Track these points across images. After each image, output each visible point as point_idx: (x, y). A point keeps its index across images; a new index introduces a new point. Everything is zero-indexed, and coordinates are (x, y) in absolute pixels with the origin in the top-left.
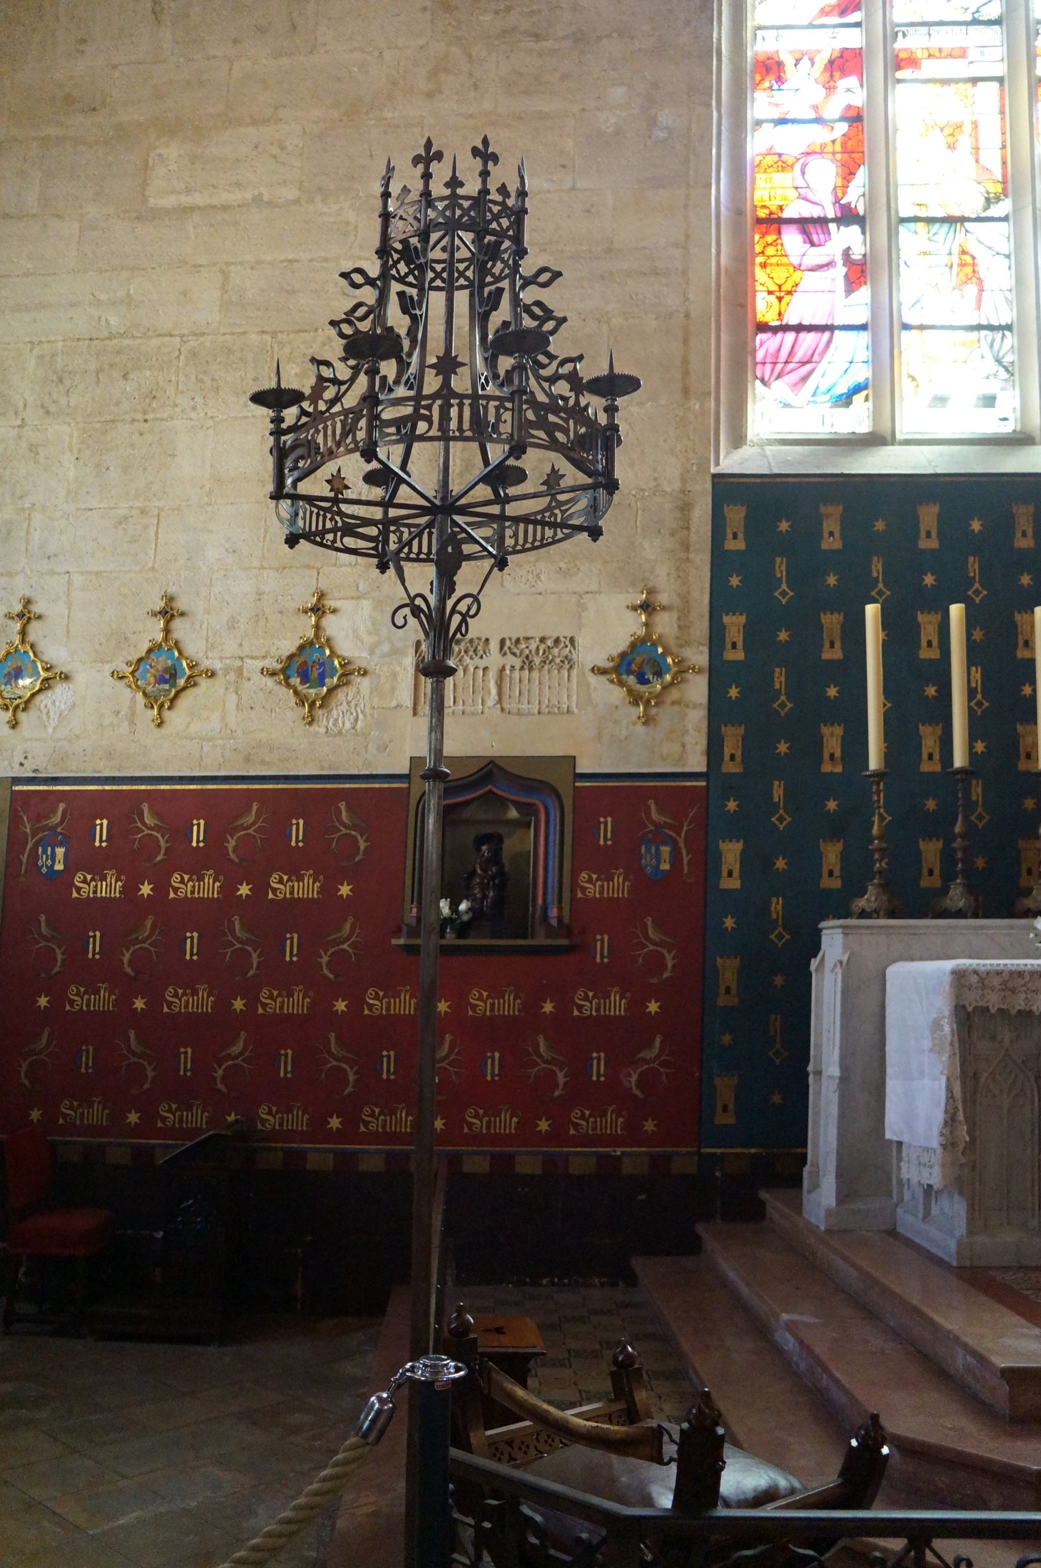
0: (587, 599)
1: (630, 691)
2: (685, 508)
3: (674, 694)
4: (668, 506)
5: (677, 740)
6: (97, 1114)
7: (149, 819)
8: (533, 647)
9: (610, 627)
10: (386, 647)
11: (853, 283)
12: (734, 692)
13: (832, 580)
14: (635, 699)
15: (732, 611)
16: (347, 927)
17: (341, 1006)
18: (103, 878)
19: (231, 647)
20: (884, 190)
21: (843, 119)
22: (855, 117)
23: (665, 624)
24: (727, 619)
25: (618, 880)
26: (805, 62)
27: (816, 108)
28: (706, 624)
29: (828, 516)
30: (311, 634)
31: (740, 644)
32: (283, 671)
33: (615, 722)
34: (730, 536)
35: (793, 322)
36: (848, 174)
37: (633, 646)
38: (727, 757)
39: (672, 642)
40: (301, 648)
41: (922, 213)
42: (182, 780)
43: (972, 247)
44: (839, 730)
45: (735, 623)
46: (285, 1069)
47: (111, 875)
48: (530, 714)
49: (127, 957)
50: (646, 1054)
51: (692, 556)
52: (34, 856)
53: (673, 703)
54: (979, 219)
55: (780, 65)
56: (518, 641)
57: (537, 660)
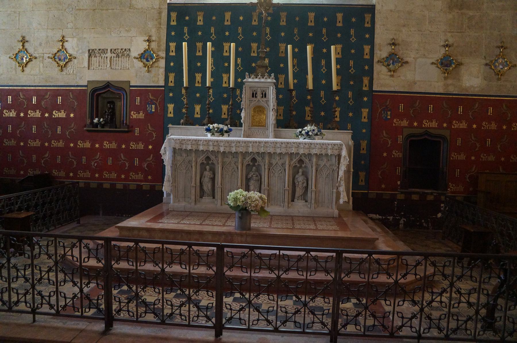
0: (133, 38)
1: (144, 64)
2: (160, 13)
3: (156, 64)
4: (156, 12)
5: (156, 77)
6: (13, 172)
7: (21, 96)
8: (119, 51)
9: (139, 46)
10: (80, 51)
12: (172, 64)
13: (200, 33)
16: (73, 125)
17: (72, 145)
18: (11, 112)
19: (40, 50)
23: (154, 45)
24: (171, 44)
25: (141, 114)
28: (165, 45)
29: (199, 15)
31: (174, 51)
33: (141, 72)
34: (172, 21)
37: (145, 51)
38: (170, 82)
39: (156, 50)
42: (30, 86)
46: (59, 161)
47: (13, 111)
48: (118, 69)
49: (18, 132)
50: (148, 159)
51: (162, 26)
53: (156, 67)
56: (115, 50)
57: (120, 55)
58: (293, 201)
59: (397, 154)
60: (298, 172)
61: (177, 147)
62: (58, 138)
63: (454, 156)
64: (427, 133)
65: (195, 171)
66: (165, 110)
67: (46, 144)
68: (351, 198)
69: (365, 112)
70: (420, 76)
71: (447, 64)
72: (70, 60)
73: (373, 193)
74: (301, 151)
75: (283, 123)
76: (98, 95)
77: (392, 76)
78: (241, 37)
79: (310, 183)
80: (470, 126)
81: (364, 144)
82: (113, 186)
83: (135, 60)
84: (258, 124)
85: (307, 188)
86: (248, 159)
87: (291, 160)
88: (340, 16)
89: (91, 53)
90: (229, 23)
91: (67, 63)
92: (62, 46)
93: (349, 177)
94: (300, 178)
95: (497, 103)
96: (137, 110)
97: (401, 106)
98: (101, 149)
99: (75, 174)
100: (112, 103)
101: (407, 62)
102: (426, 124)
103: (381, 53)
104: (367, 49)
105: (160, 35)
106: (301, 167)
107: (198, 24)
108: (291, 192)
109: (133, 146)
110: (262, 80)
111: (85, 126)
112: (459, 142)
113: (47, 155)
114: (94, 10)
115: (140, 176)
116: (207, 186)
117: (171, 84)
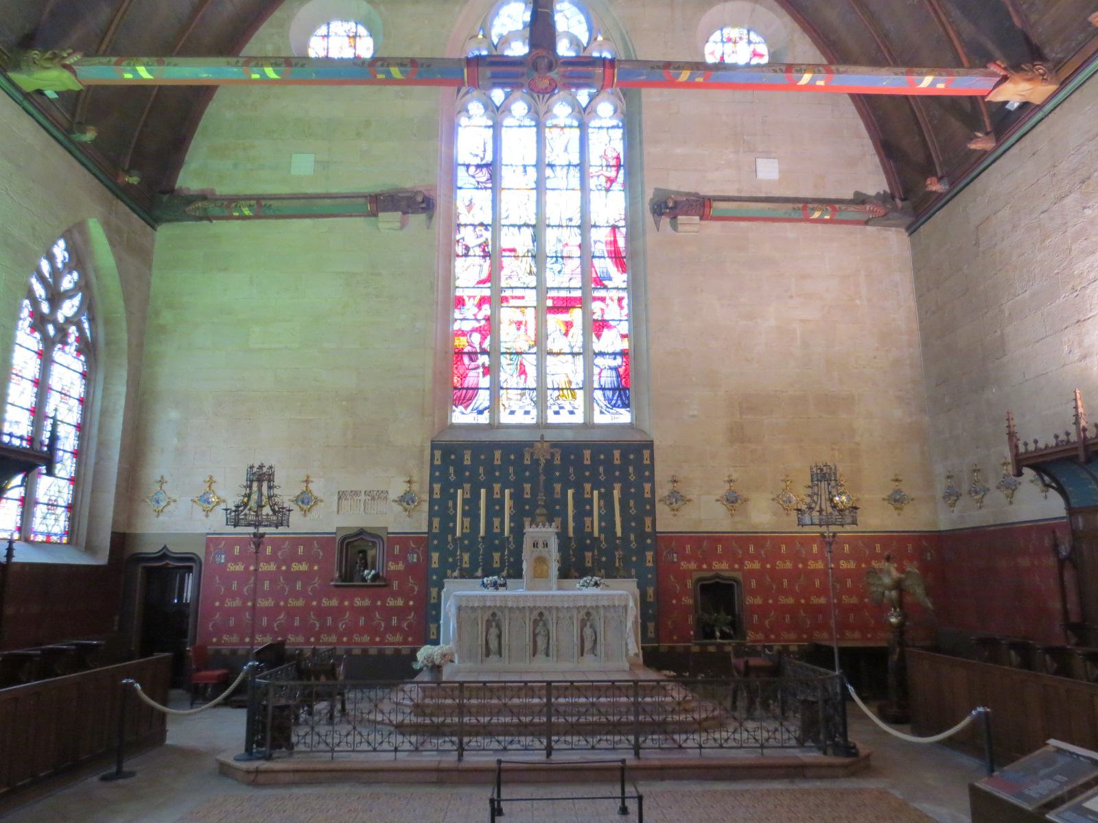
2: (422, 451)
3: (418, 508)
5: (418, 522)
6: (235, 639)
9: (398, 488)
11: (485, 374)
14: (406, 510)
20: (496, 342)
21: (484, 319)
22: (487, 319)
23: (415, 487)
26: (472, 299)
27: (475, 315)
30: (305, 489)
32: (296, 500)
35: (466, 385)
36: (484, 338)
37: (405, 494)
40: (302, 493)
41: (508, 351)
43: (525, 363)
44: (469, 519)
45: (437, 487)
50: (409, 618)
52: (214, 558)
54: (526, 353)
55: (463, 300)
58: (582, 655)
59: (688, 601)
60: (586, 625)
61: (464, 604)
62: (296, 595)
63: (750, 600)
64: (718, 576)
65: (481, 628)
66: (428, 559)
67: (282, 604)
68: (641, 651)
69: (649, 555)
70: (705, 514)
71: (733, 501)
72: (316, 503)
73: (664, 646)
74: (589, 604)
75: (564, 574)
76: (348, 544)
77: (675, 515)
78: (512, 478)
79: (598, 635)
80: (763, 566)
81: (651, 591)
82: (365, 651)
83: (393, 504)
84: (540, 575)
85: (595, 640)
86: (536, 613)
87: (579, 612)
88: (617, 453)
89: (341, 496)
90: (499, 462)
91: (311, 507)
92: (307, 487)
93: (637, 628)
94: (588, 631)
95: (789, 540)
96: (396, 559)
97: (688, 547)
98: (352, 608)
99: (318, 639)
100: (364, 552)
101: (689, 500)
102: (717, 566)
103: (662, 491)
104: (647, 487)
105: (422, 475)
106: (588, 620)
107: (465, 463)
108: (579, 646)
109: (391, 602)
110: (544, 530)
111: (332, 580)
112: (753, 583)
113: (282, 617)
114: (346, 447)
115: (399, 638)
116: (493, 645)
117: (436, 531)
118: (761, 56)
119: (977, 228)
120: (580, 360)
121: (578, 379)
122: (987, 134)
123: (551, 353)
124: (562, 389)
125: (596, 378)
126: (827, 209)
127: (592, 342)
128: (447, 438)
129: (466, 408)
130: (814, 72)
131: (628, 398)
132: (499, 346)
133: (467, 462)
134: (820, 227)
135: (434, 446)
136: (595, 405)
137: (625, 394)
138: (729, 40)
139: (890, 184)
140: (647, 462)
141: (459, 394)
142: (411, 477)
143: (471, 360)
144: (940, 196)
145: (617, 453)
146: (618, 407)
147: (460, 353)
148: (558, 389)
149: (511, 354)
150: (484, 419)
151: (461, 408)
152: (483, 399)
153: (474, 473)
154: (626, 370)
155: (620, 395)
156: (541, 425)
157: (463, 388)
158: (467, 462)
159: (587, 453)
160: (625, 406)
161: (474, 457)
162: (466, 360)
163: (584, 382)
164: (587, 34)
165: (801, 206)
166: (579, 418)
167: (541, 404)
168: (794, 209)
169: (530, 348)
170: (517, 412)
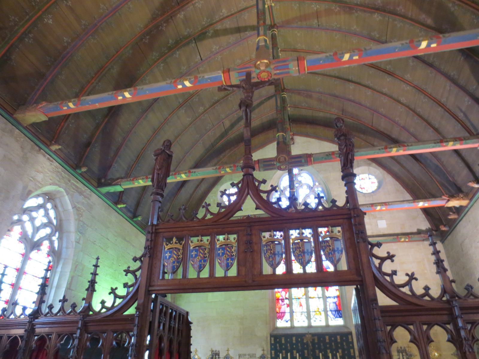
15: (273, 350)
23: (265, 352)
35: (281, 312)
45: (273, 352)
118: (374, 183)
119: (461, 244)
120: (321, 300)
121: (322, 307)
122: (454, 213)
123: (311, 298)
124: (316, 312)
125: (328, 307)
126: (406, 238)
127: (325, 293)
128: (275, 333)
129: (282, 320)
130: (381, 206)
131: (341, 314)
132: (292, 296)
133: (283, 342)
134: (405, 243)
135: (271, 336)
136: (329, 317)
137: (340, 313)
138: (362, 179)
139: (431, 226)
140: (350, 340)
141: (279, 315)
142: (264, 348)
143: (282, 302)
144: (447, 231)
145: (338, 337)
146: (338, 318)
147: (278, 299)
148: (315, 312)
149: (296, 299)
150: (288, 325)
151: (280, 320)
152: (287, 317)
153: (286, 347)
154: (339, 303)
155: (338, 313)
156: (310, 326)
157: (280, 313)
158: (283, 342)
159: (327, 337)
160: (340, 317)
161: (286, 340)
162: (280, 301)
163: (324, 309)
164: (312, 183)
165: (396, 237)
166: (323, 324)
167: (309, 318)
168: (393, 238)
169: (303, 296)
170: (300, 322)
